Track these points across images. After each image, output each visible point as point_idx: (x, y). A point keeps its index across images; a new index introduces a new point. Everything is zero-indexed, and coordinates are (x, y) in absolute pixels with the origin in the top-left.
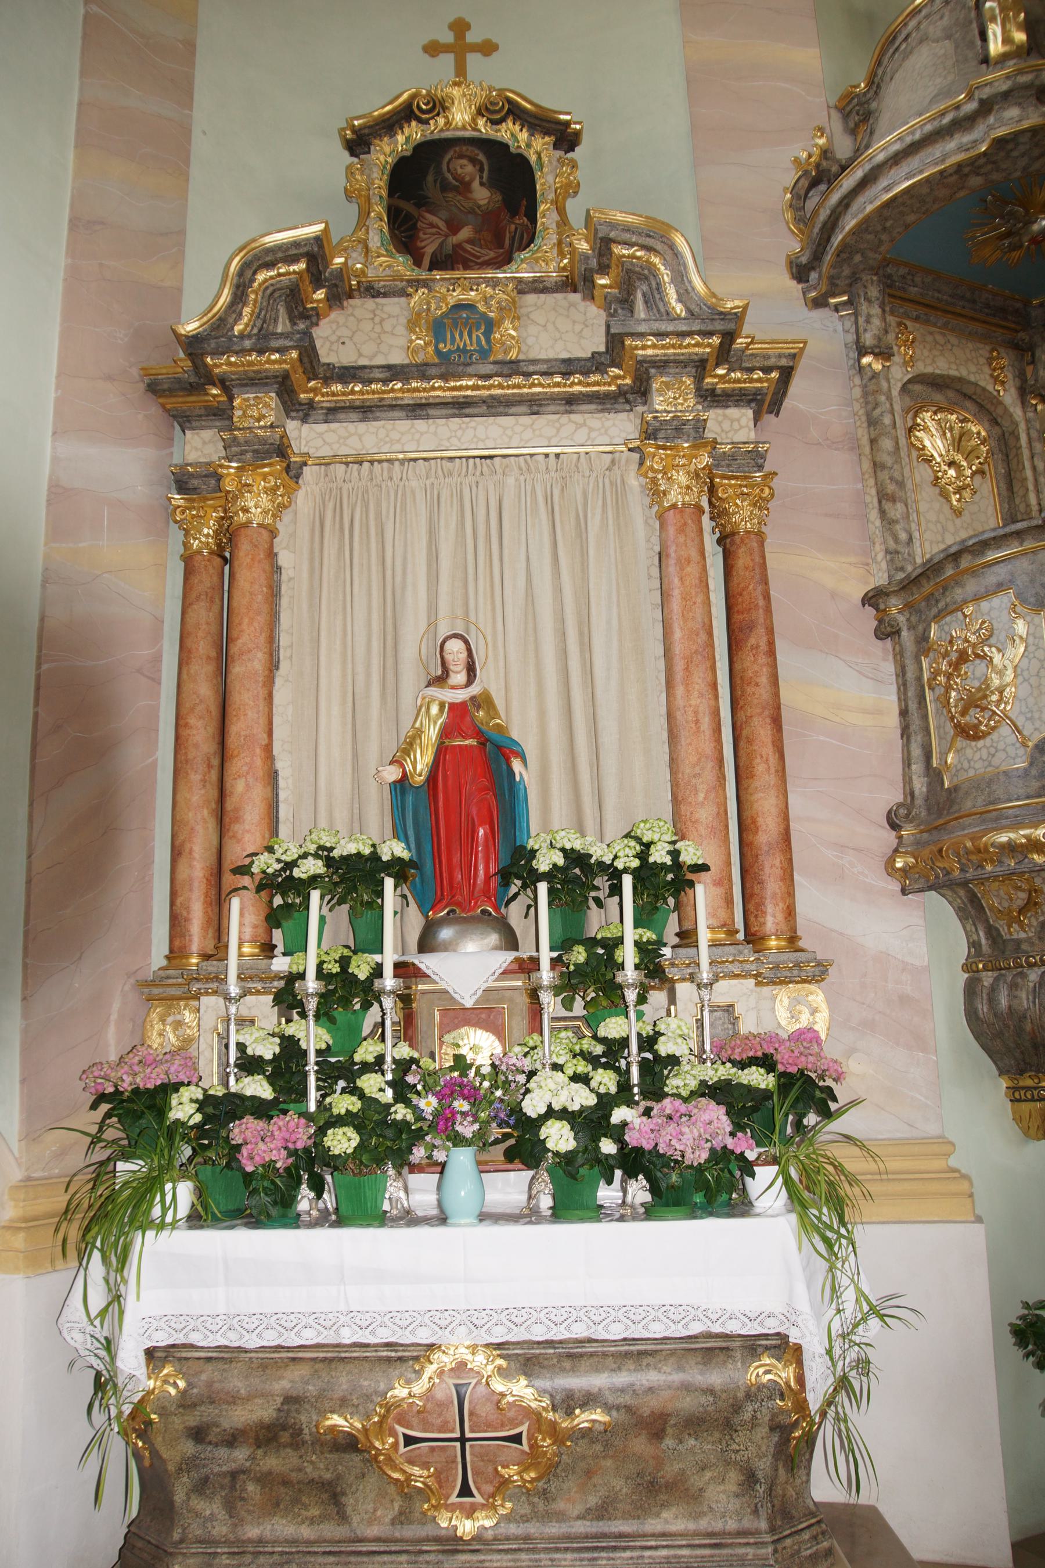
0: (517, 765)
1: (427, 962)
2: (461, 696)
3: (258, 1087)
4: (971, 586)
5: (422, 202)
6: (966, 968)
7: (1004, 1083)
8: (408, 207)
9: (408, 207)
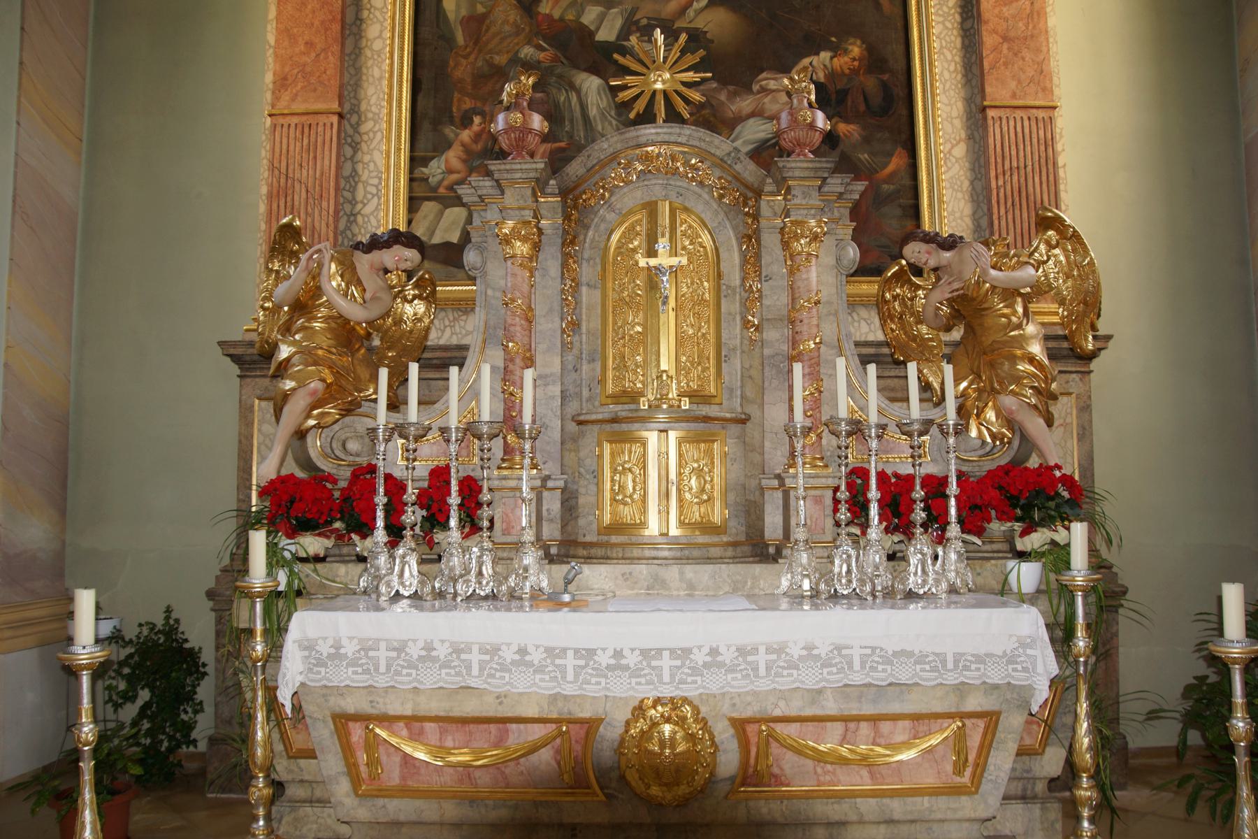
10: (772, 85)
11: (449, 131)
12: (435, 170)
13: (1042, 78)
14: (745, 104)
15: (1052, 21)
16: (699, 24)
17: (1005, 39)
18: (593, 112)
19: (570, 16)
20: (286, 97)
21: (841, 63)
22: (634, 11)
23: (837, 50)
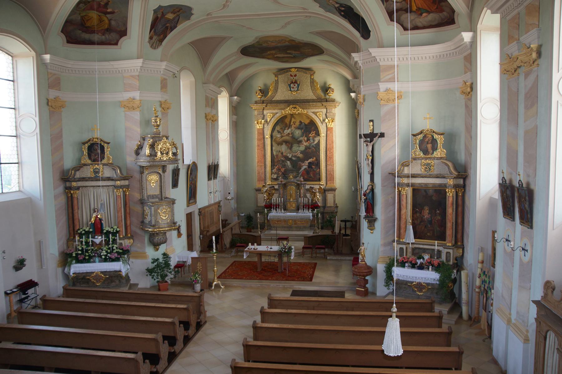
0: (102, 222)
1: (94, 240)
2: (97, 214)
3: (80, 252)
5: (92, 152)
8: (90, 152)
9: (90, 152)
12: (273, 171)
13: (333, 162)
14: (303, 164)
15: (334, 155)
16: (299, 156)
17: (329, 158)
21: (313, 160)
23: (313, 158)
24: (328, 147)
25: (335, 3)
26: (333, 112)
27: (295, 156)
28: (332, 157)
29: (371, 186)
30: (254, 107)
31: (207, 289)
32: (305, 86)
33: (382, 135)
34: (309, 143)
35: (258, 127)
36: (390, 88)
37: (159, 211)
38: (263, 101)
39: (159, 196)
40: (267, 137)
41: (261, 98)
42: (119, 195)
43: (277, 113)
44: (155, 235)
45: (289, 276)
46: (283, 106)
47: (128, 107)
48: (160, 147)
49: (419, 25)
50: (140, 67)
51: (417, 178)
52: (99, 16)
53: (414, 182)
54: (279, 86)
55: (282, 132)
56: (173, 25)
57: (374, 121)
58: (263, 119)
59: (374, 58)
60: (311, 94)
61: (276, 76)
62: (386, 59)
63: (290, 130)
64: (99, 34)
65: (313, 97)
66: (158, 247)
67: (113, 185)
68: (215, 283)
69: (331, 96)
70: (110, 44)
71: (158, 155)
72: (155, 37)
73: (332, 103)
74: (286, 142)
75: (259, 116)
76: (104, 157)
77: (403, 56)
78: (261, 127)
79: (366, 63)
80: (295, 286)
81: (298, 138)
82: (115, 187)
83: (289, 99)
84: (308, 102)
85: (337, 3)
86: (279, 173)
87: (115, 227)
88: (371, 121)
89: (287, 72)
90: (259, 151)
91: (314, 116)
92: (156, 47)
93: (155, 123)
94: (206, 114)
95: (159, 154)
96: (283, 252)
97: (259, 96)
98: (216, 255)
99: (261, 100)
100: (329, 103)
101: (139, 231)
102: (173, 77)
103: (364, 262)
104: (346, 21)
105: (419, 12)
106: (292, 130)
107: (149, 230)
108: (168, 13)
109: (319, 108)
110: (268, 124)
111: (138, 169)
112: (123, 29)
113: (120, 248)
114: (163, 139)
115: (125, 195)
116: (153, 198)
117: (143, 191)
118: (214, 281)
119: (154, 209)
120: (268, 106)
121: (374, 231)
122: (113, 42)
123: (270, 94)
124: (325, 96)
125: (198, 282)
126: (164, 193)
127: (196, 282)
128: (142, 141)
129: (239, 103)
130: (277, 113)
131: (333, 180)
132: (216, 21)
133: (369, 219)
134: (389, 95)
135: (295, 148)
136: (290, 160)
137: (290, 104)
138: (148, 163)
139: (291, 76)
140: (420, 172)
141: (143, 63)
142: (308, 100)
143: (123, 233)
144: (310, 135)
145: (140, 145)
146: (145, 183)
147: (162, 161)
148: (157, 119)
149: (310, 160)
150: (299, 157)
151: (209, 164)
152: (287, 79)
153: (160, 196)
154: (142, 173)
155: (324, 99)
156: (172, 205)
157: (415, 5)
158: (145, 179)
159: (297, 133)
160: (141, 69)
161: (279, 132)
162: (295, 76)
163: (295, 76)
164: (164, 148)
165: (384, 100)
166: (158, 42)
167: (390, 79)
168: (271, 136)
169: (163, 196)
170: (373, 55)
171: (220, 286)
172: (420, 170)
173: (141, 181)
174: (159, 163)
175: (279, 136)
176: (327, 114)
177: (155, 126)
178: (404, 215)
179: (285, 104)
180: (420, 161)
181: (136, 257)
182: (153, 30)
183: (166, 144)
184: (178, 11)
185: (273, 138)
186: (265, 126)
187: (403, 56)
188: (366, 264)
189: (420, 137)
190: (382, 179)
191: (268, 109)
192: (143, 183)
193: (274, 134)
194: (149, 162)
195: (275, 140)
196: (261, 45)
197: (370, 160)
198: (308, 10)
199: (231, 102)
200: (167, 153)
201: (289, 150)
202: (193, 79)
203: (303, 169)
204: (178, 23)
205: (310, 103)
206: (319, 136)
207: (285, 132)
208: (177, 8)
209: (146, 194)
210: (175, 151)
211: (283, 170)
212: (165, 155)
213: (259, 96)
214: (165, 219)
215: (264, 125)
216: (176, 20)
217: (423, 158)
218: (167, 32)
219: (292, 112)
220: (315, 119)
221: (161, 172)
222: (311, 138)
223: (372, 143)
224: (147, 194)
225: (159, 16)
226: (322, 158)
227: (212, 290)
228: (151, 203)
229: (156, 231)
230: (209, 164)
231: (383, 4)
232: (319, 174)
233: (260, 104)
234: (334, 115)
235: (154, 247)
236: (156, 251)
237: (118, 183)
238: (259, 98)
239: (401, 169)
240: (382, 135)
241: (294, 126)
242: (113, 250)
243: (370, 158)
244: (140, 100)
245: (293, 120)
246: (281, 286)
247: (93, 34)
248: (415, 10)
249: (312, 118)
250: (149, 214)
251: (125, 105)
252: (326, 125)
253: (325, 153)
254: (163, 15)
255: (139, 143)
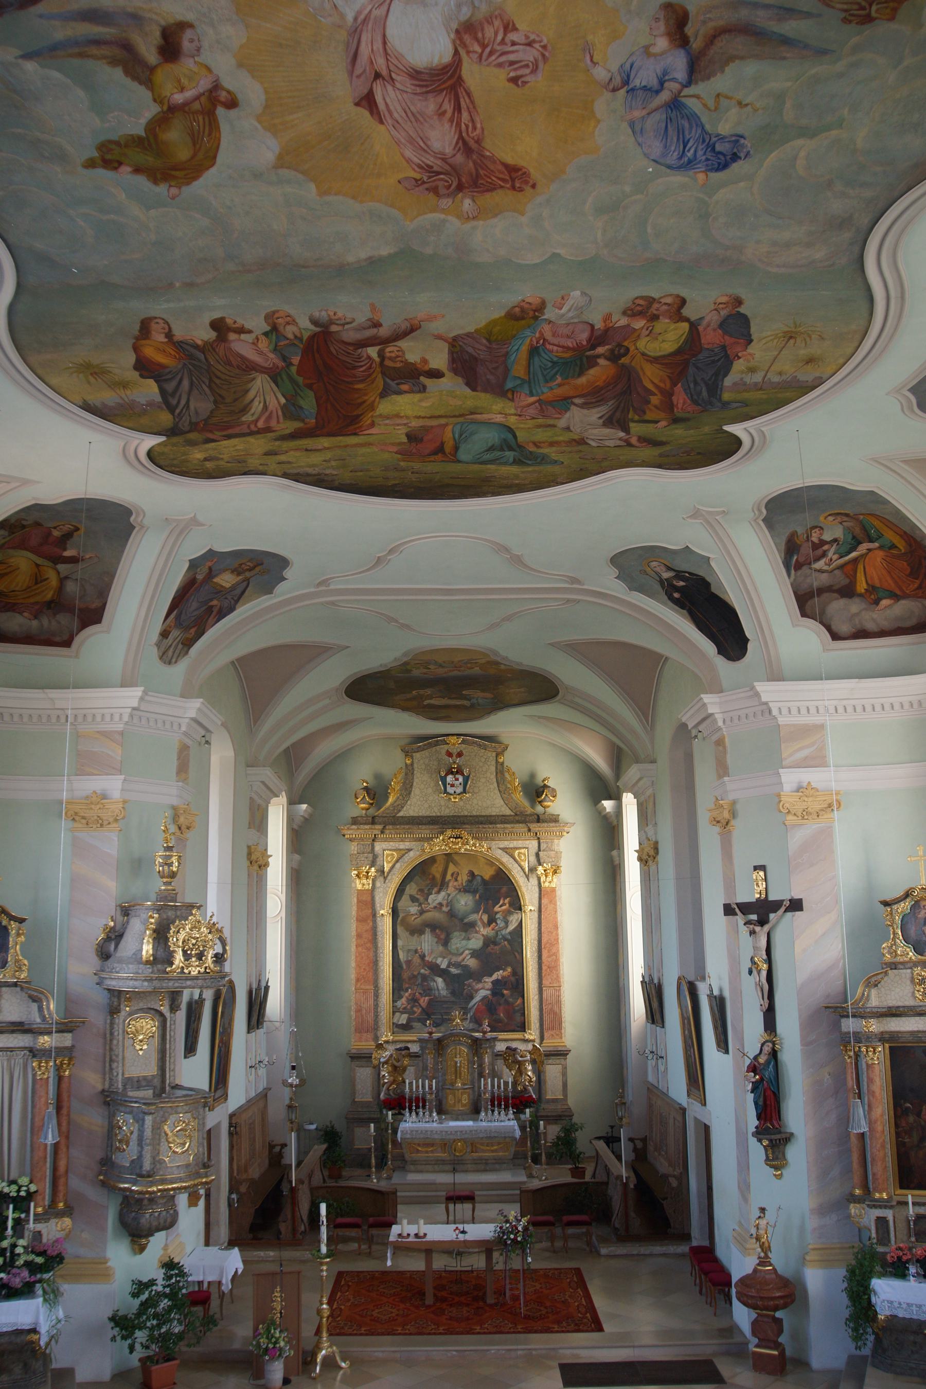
4: (123, 1109)
6: (121, 1204)
7: (130, 1238)
10: (487, 980)
11: (402, 993)
12: (399, 1004)
13: (558, 979)
14: (480, 986)
17: (549, 967)
18: (440, 988)
19: (434, 961)
20: (359, 984)
21: (505, 974)
22: (451, 959)
23: (504, 970)
24: (544, 940)
25: (664, 569)
26: (556, 848)
27: (457, 965)
28: (555, 967)
29: (770, 1045)
30: (352, 832)
31: (298, 1375)
32: (483, 780)
33: (796, 905)
34: (493, 929)
35: (359, 887)
36: (809, 783)
37: (166, 1127)
38: (373, 818)
39: (156, 1080)
40: (382, 912)
41: (367, 809)
42: (46, 1077)
43: (409, 850)
44: (146, 1202)
45: (527, 1317)
46: (428, 832)
47: (83, 818)
48: (182, 935)
49: (870, 626)
50: (129, 710)
51: (904, 1019)
52: (37, 565)
53: (897, 1029)
54: (416, 781)
55: (421, 899)
56: (226, 605)
57: (768, 869)
58: (373, 864)
59: (764, 707)
60: (499, 802)
61: (407, 753)
62: (794, 711)
63: (443, 894)
64: (25, 614)
65: (503, 809)
66: (144, 1241)
67: (27, 1045)
68: (324, 1352)
69: (548, 807)
70: (49, 642)
71: (177, 962)
72: (175, 633)
73: (553, 824)
74: (433, 927)
75: (362, 857)
76: (6, 962)
77: (835, 703)
78: (367, 887)
79: (736, 721)
80: (561, 1351)
81: (465, 917)
82: (33, 1052)
83: (442, 814)
84: (491, 823)
85: (669, 569)
86: (415, 1009)
87: (24, 1181)
88: (756, 868)
89: (437, 744)
90: (360, 949)
91: (506, 859)
92: (174, 660)
93: (166, 868)
94: (249, 847)
95: (179, 957)
96: (509, 1242)
97: (363, 805)
98: (327, 1263)
99: (367, 816)
100: (546, 824)
101: (93, 1193)
102: (200, 744)
103: (771, 1265)
104: (683, 616)
105: (872, 597)
106: (449, 895)
107: (133, 1188)
108: (225, 570)
109: (519, 836)
110: (385, 878)
111: (101, 998)
112: (93, 606)
113: (38, 1249)
114: (192, 914)
115: (60, 1079)
116: (138, 1088)
117: (114, 1065)
118: (318, 1347)
119: (154, 1121)
120: (387, 832)
121: (785, 1172)
122: (58, 639)
123: (391, 800)
124: (533, 806)
125: (280, 1355)
126: (172, 1073)
127: (274, 1353)
128: (120, 918)
129: (307, 820)
130: (409, 850)
131: (560, 1029)
132: (333, 603)
133: (773, 1137)
134: (806, 799)
135: (457, 942)
136: (443, 973)
137: (445, 827)
138: (146, 984)
139: (449, 754)
140: (910, 1002)
141: (142, 699)
142: (491, 816)
143: (44, 1199)
144: (497, 909)
145: (113, 929)
146: (121, 1043)
147: (187, 979)
148: (171, 856)
149: (498, 975)
150: (466, 966)
151: (250, 985)
152: (436, 763)
153: (157, 1082)
154: (114, 1011)
155: (531, 815)
156: (201, 1110)
157: (863, 579)
158: (121, 1031)
159: (463, 903)
160: (131, 716)
161: (413, 899)
162: (460, 755)
163: (460, 755)
164: (194, 941)
165: (795, 814)
166: (180, 646)
167: (806, 758)
168: (393, 911)
169: (168, 1082)
170: (764, 699)
171: (337, 1362)
172: (910, 995)
173: (109, 1038)
174: (177, 985)
175: (414, 909)
176: (541, 854)
177: (162, 877)
178: (879, 1123)
179: (431, 827)
180: (909, 971)
181: (77, 1278)
182: (175, 612)
183: (200, 929)
184: (250, 570)
185: (398, 916)
186: (378, 884)
187: (835, 703)
188: (774, 1269)
189: (905, 906)
190: (800, 1025)
191: (386, 840)
192: (115, 1042)
193: (401, 905)
194: (151, 980)
195: (405, 924)
196: (409, 671)
197: (764, 974)
198: (584, 585)
199: (290, 819)
200: (200, 956)
201: (441, 948)
202: (230, 753)
203: (478, 998)
204: (241, 601)
205: (498, 826)
206: (520, 909)
207: (430, 900)
208: (249, 561)
209: (120, 1076)
210: (218, 949)
211: (424, 1001)
212: (194, 959)
213: (363, 805)
214: (183, 1153)
215: (374, 881)
216: (238, 591)
217: (915, 964)
218: (209, 617)
219: (450, 848)
220: (510, 866)
221: (165, 1010)
222: (498, 916)
223: (766, 928)
224: (123, 1074)
225: (200, 577)
226: (530, 969)
227: (314, 1379)
228: (144, 1104)
229: (153, 1192)
230: (250, 985)
231: (789, 575)
232: (522, 1011)
233: (366, 827)
234: (558, 855)
235: (133, 1242)
236: (135, 1253)
237: (45, 1041)
238: (363, 809)
239: (863, 994)
240: (796, 905)
241: (456, 883)
242: (14, 1256)
243: (765, 966)
244: (125, 802)
245: (452, 869)
246: (520, 1352)
247: (9, 614)
248: (863, 591)
249: (502, 863)
250: (135, 1136)
251: (76, 814)
252: (536, 882)
253: (536, 954)
254: (210, 574)
255: (112, 924)
